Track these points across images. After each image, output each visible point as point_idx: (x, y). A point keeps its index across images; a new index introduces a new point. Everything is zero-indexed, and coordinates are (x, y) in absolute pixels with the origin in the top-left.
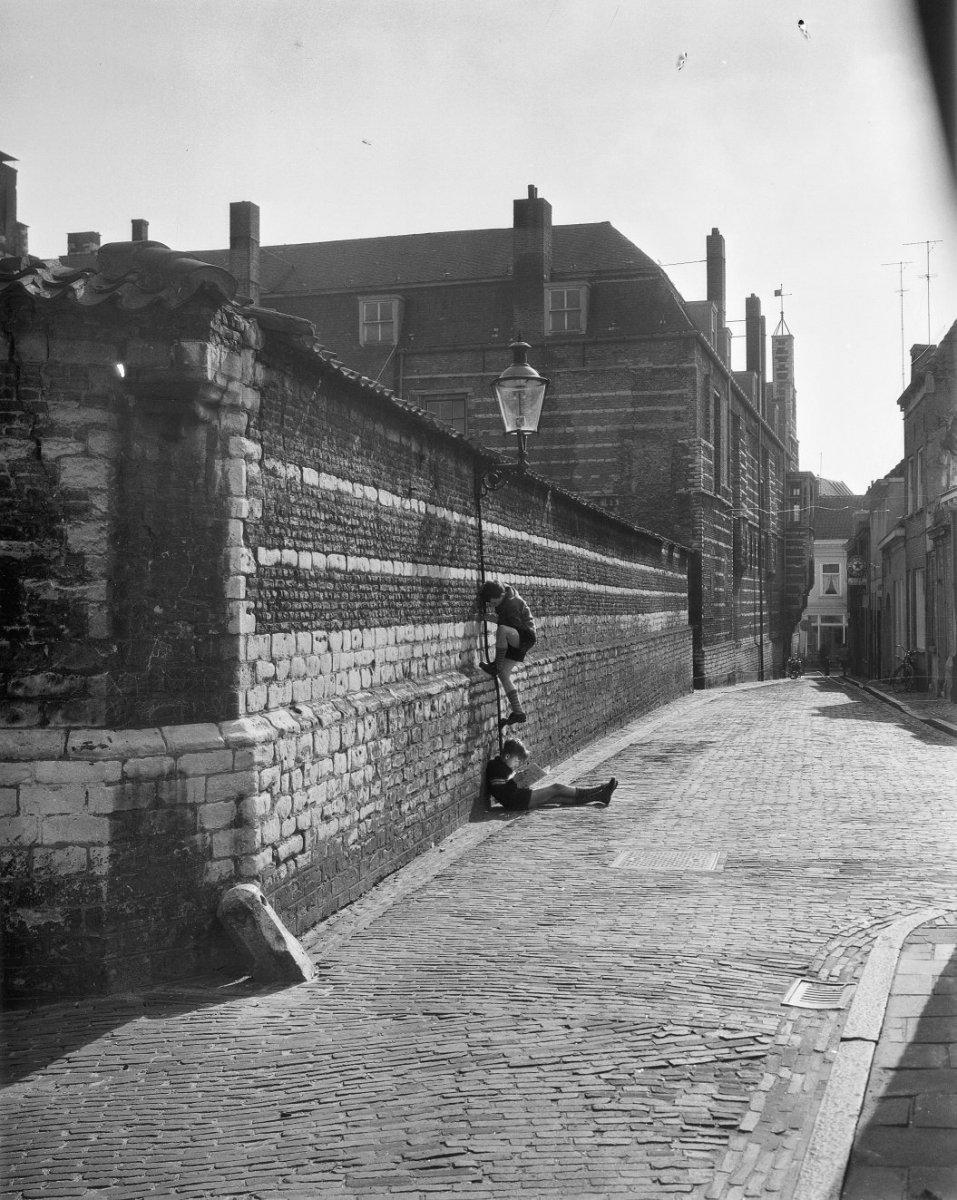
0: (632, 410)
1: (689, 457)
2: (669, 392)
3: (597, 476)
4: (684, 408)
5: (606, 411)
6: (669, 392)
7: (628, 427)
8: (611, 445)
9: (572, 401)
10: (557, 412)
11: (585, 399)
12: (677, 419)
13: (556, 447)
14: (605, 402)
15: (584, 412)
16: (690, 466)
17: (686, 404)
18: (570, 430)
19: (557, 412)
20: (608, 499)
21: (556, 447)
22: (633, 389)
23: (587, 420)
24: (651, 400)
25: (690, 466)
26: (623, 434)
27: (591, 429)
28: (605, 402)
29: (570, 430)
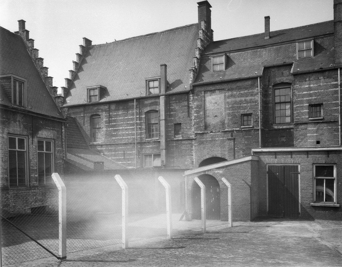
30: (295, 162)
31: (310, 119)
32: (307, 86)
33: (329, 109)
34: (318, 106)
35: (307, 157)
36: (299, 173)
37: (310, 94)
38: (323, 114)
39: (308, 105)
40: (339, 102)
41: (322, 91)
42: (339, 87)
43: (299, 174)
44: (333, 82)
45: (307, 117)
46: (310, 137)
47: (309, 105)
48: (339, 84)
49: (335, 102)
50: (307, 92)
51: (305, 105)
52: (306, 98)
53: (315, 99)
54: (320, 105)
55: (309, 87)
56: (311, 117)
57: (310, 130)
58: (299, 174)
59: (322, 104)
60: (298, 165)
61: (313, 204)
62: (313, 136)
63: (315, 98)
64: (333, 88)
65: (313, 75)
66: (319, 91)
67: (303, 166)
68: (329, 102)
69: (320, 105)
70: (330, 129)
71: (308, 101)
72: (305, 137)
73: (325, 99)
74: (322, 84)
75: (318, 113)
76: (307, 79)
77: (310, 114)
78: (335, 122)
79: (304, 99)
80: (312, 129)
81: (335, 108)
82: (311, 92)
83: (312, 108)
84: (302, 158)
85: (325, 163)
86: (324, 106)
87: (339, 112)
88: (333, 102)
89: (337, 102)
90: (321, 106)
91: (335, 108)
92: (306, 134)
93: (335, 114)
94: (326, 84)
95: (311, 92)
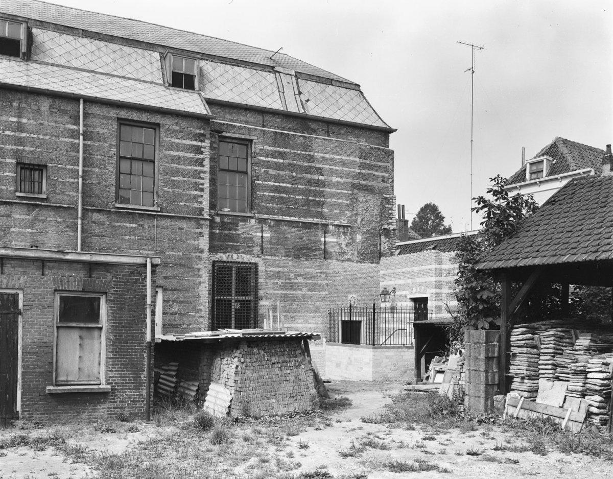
0: (359, 171)
1: (390, 206)
2: (379, 164)
3: (338, 211)
4: (387, 175)
5: (344, 169)
6: (379, 164)
7: (357, 181)
8: (346, 192)
9: (324, 158)
10: (313, 164)
11: (331, 159)
12: (383, 181)
13: (313, 188)
14: (343, 163)
15: (331, 167)
16: (390, 212)
17: (388, 172)
18: (321, 178)
19: (313, 164)
20: (344, 227)
21: (313, 188)
22: (360, 158)
23: (332, 173)
24: (370, 167)
25: (390, 212)
26: (354, 186)
27: (335, 179)
28: (343, 163)
29: (321, 178)
30: (10, 285)
31: (18, 194)
32: (15, 119)
33: (60, 180)
34: (37, 170)
35: (41, 273)
36: (20, 314)
37: (21, 138)
38: (47, 190)
39: (14, 161)
40: (80, 168)
41: (47, 137)
42: (81, 137)
43: (20, 316)
44: (68, 123)
45: (12, 189)
46: (18, 234)
47: (18, 163)
48: (81, 132)
49: (72, 167)
50: (12, 133)
51: (8, 161)
52: (10, 146)
53: (31, 152)
54: (40, 168)
55: (19, 123)
56: (21, 192)
57: (16, 220)
58: (20, 316)
59: (46, 166)
60: (18, 291)
61: (51, 388)
62: (23, 234)
63: (32, 149)
64: (68, 137)
65: (27, 98)
66: (41, 137)
67: (30, 296)
68: (60, 166)
69: (41, 168)
70: (60, 222)
71: (17, 154)
72: (5, 235)
73: (51, 156)
74: (46, 123)
75: (37, 184)
76: (15, 104)
77: (20, 183)
78: (71, 209)
79: (7, 147)
80: (23, 217)
81: (72, 180)
82: (23, 135)
83: (23, 171)
84: (28, 275)
85: (83, 291)
86: (50, 170)
87: (78, 190)
88: (68, 167)
89: (76, 167)
90: (42, 170)
91: (72, 180)
92: (10, 227)
93: (71, 193)
94: (54, 124)
95: (23, 135)
